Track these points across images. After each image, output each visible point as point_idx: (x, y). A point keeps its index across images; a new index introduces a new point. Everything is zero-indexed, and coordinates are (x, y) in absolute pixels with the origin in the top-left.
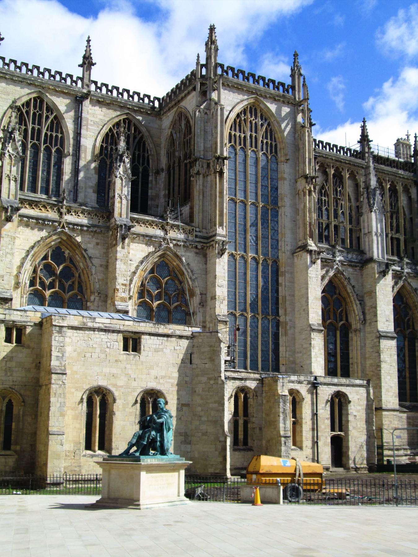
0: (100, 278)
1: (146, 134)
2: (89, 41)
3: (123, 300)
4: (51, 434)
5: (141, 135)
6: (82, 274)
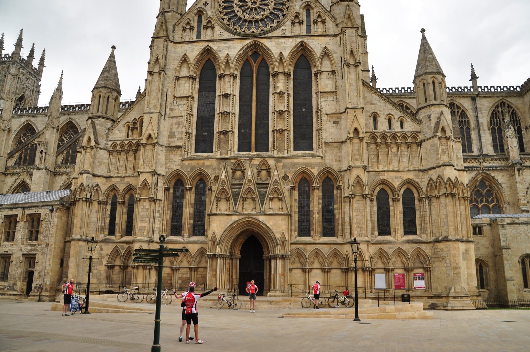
0: (508, 194)
1: (515, 108)
2: (472, 66)
3: (524, 204)
4: (509, 280)
5: (512, 109)
6: (497, 193)
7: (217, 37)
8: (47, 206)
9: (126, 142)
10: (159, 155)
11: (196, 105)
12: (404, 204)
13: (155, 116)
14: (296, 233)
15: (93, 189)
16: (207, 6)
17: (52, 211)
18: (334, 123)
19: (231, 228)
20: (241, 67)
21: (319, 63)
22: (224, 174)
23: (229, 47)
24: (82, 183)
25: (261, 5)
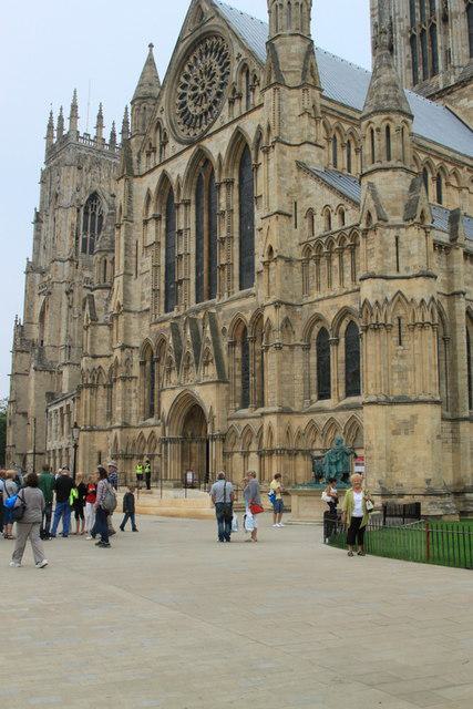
11: (163, 252)
12: (347, 347)
13: (121, 278)
14: (238, 405)
17: (73, 400)
19: (175, 405)
20: (194, 187)
21: (253, 156)
23: (179, 165)
25: (210, 85)
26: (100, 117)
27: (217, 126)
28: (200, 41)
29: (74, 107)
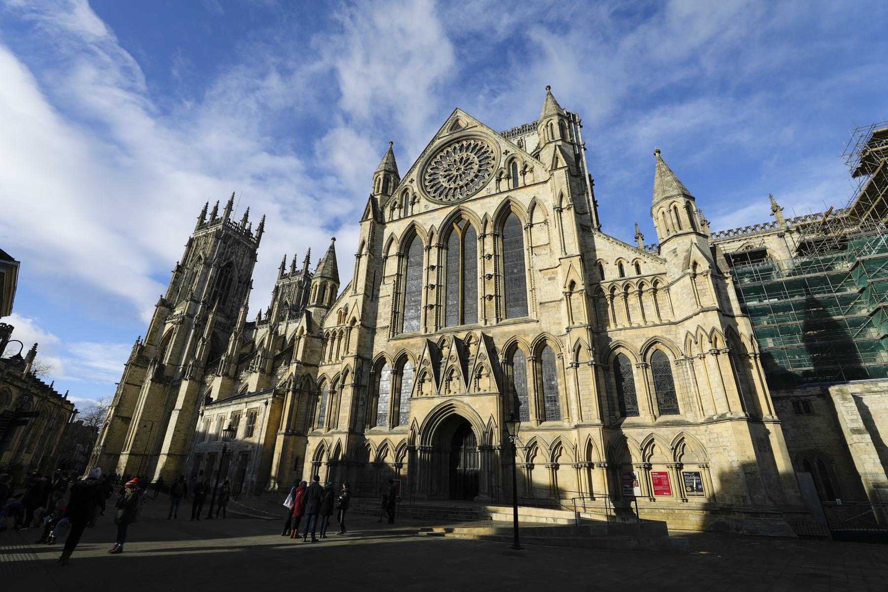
7: (423, 210)
8: (263, 399)
9: (338, 328)
10: (365, 338)
13: (360, 298)
15: (304, 379)
16: (415, 183)
17: (266, 404)
18: (549, 279)
22: (427, 351)
24: (292, 373)
26: (246, 215)
27: (483, 193)
28: (458, 140)
29: (231, 203)
